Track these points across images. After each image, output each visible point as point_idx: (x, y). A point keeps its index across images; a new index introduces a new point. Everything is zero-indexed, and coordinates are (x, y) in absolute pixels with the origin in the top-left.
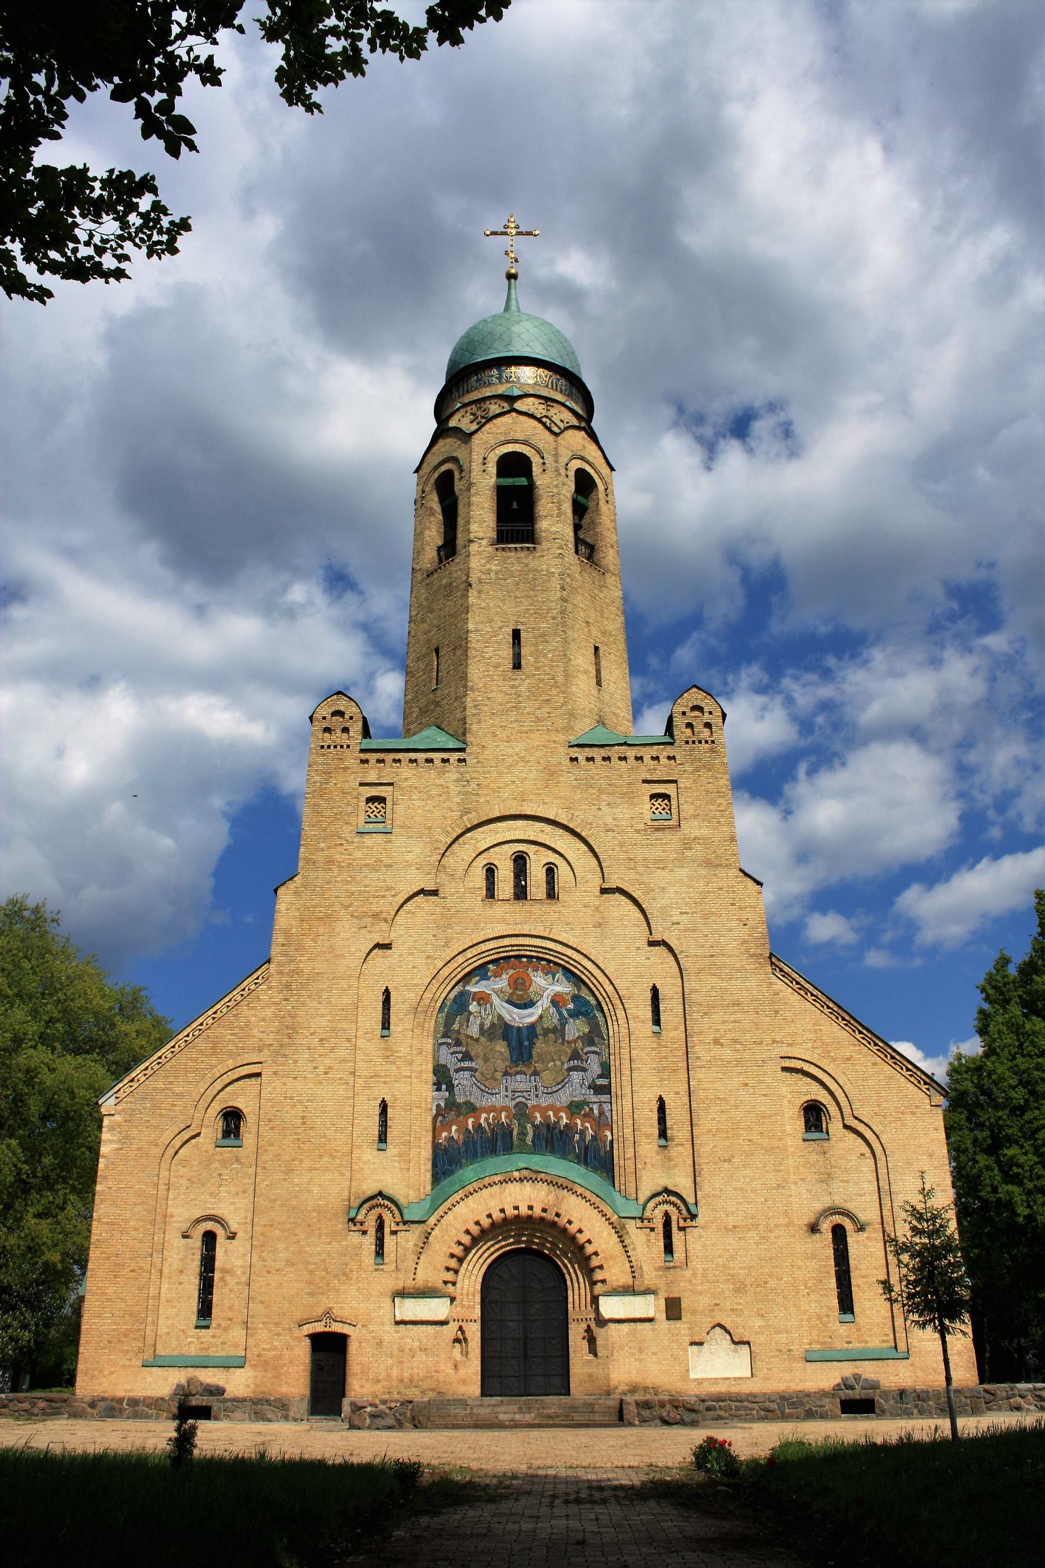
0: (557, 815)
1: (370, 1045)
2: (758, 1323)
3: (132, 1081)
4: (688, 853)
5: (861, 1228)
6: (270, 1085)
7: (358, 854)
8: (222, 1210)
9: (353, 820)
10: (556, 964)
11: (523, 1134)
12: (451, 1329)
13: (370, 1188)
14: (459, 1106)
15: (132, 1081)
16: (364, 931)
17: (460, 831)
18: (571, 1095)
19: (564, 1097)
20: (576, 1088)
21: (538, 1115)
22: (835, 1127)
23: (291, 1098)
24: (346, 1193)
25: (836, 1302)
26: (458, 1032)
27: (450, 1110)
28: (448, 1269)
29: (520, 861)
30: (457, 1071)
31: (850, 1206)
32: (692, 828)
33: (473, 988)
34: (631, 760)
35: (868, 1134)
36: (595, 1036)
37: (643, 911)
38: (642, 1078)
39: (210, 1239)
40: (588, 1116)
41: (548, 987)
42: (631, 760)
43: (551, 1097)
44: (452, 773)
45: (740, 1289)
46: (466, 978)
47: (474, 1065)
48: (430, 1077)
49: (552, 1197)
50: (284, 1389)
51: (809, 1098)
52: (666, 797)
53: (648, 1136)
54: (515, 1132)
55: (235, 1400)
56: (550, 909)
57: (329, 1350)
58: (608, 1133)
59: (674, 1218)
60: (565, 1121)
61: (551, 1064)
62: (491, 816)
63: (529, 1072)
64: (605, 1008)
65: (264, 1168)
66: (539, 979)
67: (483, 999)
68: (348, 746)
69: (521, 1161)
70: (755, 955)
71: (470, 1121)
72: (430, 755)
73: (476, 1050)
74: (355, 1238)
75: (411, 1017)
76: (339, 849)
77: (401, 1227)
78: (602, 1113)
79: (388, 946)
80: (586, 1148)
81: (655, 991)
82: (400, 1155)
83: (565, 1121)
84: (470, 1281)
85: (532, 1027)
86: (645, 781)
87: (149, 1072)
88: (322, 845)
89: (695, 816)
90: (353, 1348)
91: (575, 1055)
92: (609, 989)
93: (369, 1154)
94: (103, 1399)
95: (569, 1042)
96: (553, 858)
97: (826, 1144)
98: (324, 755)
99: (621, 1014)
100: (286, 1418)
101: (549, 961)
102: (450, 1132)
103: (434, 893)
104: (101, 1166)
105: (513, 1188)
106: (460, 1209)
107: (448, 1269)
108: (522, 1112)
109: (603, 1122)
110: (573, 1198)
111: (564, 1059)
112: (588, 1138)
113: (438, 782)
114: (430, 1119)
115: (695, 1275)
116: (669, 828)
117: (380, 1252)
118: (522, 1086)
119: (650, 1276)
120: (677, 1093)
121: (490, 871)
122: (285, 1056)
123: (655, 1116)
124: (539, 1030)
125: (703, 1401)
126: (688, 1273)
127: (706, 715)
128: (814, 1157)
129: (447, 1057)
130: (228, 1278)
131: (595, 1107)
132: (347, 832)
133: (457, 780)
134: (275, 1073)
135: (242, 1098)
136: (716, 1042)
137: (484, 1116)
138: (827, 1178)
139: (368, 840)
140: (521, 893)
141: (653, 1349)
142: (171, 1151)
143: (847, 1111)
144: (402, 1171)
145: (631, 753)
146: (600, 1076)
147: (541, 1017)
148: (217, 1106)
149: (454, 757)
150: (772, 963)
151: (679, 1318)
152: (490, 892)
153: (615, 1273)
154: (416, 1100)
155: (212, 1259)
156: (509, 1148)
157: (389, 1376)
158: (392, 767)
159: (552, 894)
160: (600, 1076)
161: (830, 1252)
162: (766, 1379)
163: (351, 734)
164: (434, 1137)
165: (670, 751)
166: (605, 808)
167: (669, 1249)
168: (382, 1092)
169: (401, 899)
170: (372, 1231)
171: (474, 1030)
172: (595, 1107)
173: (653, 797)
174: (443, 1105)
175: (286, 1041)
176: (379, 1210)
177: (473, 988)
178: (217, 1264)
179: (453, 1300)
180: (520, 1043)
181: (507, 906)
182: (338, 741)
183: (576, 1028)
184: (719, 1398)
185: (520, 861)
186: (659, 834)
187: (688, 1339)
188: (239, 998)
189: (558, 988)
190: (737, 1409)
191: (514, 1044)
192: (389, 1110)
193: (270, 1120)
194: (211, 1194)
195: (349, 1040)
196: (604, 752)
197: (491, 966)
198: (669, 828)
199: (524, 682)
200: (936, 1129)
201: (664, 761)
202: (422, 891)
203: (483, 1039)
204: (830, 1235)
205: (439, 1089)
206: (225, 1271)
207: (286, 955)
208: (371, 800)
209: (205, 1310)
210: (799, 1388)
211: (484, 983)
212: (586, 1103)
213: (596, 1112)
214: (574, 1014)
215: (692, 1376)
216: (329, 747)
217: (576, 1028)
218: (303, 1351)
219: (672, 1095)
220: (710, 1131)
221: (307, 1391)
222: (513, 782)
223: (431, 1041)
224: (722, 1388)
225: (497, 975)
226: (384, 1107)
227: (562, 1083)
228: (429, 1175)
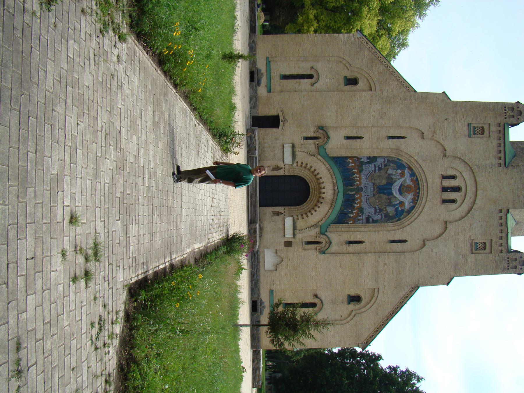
0: (477, 204)
1: (384, 133)
2: (283, 274)
3: (367, 43)
4: (461, 257)
6: (367, 95)
7: (459, 124)
8: (321, 81)
9: (474, 122)
10: (416, 203)
11: (351, 190)
12: (281, 165)
13: (331, 134)
14: (361, 166)
15: (367, 43)
16: (428, 128)
17: (470, 165)
18: (366, 208)
19: (365, 206)
20: (369, 210)
21: (358, 196)
22: (352, 306)
23: (363, 103)
24: (328, 125)
26: (390, 166)
27: (359, 162)
28: (302, 163)
29: (457, 189)
30: (375, 165)
31: (323, 310)
32: (471, 258)
33: (406, 171)
34: (500, 235)
35: (349, 319)
36: (388, 218)
37: (437, 238)
38: (371, 235)
39: (310, 77)
40: (358, 215)
41: (407, 199)
42: (500, 235)
43: (365, 202)
44: (495, 161)
46: (410, 168)
47: (377, 171)
48: (372, 156)
49: (328, 201)
50: (260, 107)
51: (363, 298)
52: (485, 249)
53: (350, 237)
54: (352, 187)
55: (256, 90)
56: (438, 201)
57: (272, 122)
58: (351, 222)
59: (320, 245)
60: (356, 206)
61: (377, 201)
62: (477, 177)
63: (374, 192)
64: (398, 222)
65: (337, 95)
66: (410, 196)
67: (402, 175)
68: (506, 118)
69: (341, 190)
70: (419, 280)
71: (356, 171)
72: (502, 152)
73: (383, 172)
74: (312, 129)
75: (394, 147)
76: (462, 117)
77: (317, 146)
78: (359, 220)
79: (423, 138)
80: (346, 214)
81: (405, 241)
82: (343, 144)
83: (356, 206)
84: (298, 172)
85: (392, 194)
86: (491, 240)
87: (370, 49)
88: (463, 110)
89: (476, 260)
90: (274, 130)
91: (381, 210)
92: (406, 223)
93: (343, 133)
94: (255, 45)
95: (386, 208)
96: (459, 202)
97: (346, 303)
98: (502, 108)
99: (396, 227)
100: (251, 108)
101: (417, 200)
102: (352, 163)
103: (445, 156)
104: (335, 35)
107: (302, 163)
108: (359, 190)
109: (355, 220)
110: (328, 208)
111: (380, 206)
112: (350, 215)
113: (491, 156)
114: (356, 156)
115: (300, 252)
116: (472, 249)
117: (307, 138)
118: (369, 190)
119: (299, 236)
120: (366, 248)
121: (453, 177)
122: (379, 100)
123: (357, 240)
124: (390, 196)
125: (257, 253)
126: (300, 250)
127: (520, 267)
128: (341, 298)
129: (380, 161)
130: (297, 84)
131: (361, 217)
132: (469, 120)
133: (492, 164)
134: (372, 96)
136: (385, 264)
137: (358, 176)
138: (333, 302)
139: (466, 128)
140: (445, 189)
141: (274, 236)
142: (341, 60)
143: (358, 311)
144: (337, 145)
145: (503, 235)
146: (373, 219)
147: (395, 197)
148: (358, 76)
149: (502, 162)
150: (415, 287)
151: (285, 246)
152: (444, 177)
153: (300, 224)
154: (364, 149)
155: (304, 78)
156: (345, 185)
157: (265, 143)
158: (497, 137)
159: (444, 201)
160: (373, 219)
161: (307, 302)
163: (511, 119)
164: (350, 157)
165: (504, 251)
167: (309, 243)
168: (366, 137)
169: (442, 141)
170: (315, 135)
171: (390, 171)
172: (361, 217)
173: (485, 243)
174: (362, 160)
175: (384, 100)
176: (323, 137)
177: (406, 171)
178: (302, 80)
179: (292, 165)
180: (386, 189)
181: (439, 184)
182: (508, 114)
183: (391, 210)
185: (457, 189)
186: (469, 245)
187: (278, 248)
188: (400, 81)
189: (407, 204)
190: (255, 265)
191: (385, 187)
192: (359, 140)
193: (354, 96)
194: (326, 76)
195: (385, 124)
196: (504, 223)
197: (415, 178)
198: (472, 249)
200: (350, 344)
201: (500, 248)
202: (445, 150)
203: (387, 175)
204: (312, 302)
205: (368, 158)
206: (300, 83)
207: (418, 98)
208: (483, 128)
209: (285, 77)
211: (409, 175)
212: (363, 214)
213: (359, 218)
214: (396, 210)
215: (265, 250)
216: (505, 110)
217: (391, 210)
218: (272, 112)
219: (365, 246)
220: (352, 260)
221: (260, 115)
222: (491, 186)
223: (386, 155)
224: (261, 260)
225: (412, 180)
226: (360, 138)
227: (370, 205)
228: (335, 156)
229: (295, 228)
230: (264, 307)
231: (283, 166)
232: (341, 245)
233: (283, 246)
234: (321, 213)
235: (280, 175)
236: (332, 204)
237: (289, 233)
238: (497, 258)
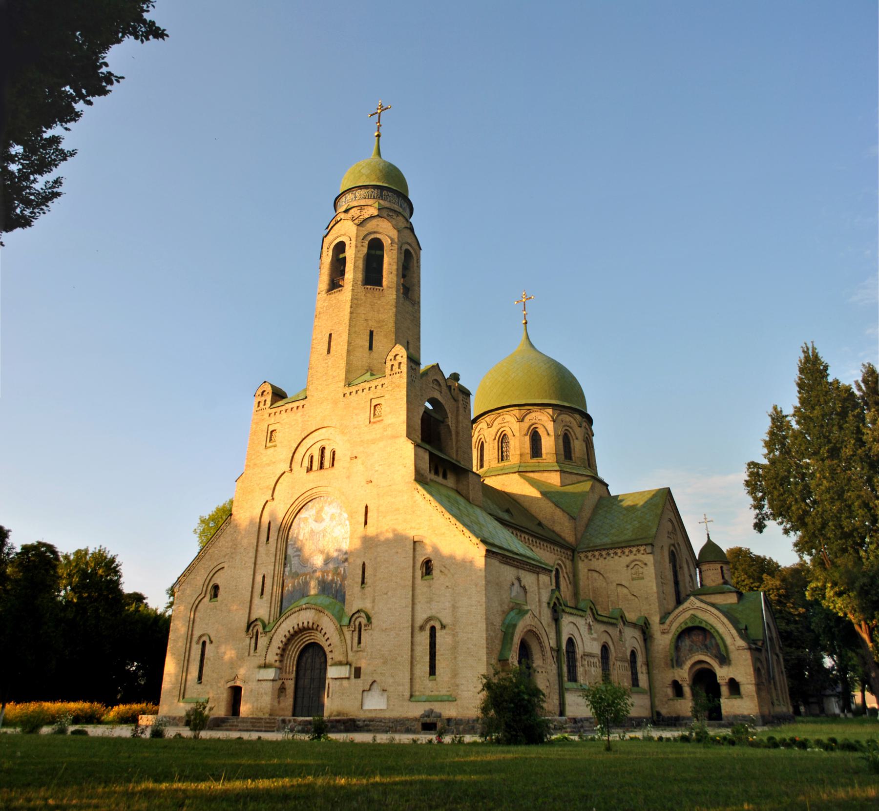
2: (391, 680)
5: (443, 627)
22: (436, 572)
25: (428, 669)
29: (323, 450)
31: (438, 615)
39: (204, 643)
45: (385, 662)
53: (357, 583)
56: (333, 470)
81: (367, 507)
105: (302, 612)
106: (284, 625)
123: (361, 572)
126: (365, 654)
135: (218, 580)
138: (430, 601)
140: (321, 467)
148: (211, 584)
162: (392, 710)
166: (354, 417)
184: (372, 720)
199: (331, 359)
210: (405, 716)
224: (373, 715)
229: (340, 664)
230: (432, 711)
231: (281, 682)
232: (364, 594)
233: (359, 681)
234: (328, 624)
235: (293, 686)
236: (320, 611)
237: (344, 671)
238: (390, 388)
